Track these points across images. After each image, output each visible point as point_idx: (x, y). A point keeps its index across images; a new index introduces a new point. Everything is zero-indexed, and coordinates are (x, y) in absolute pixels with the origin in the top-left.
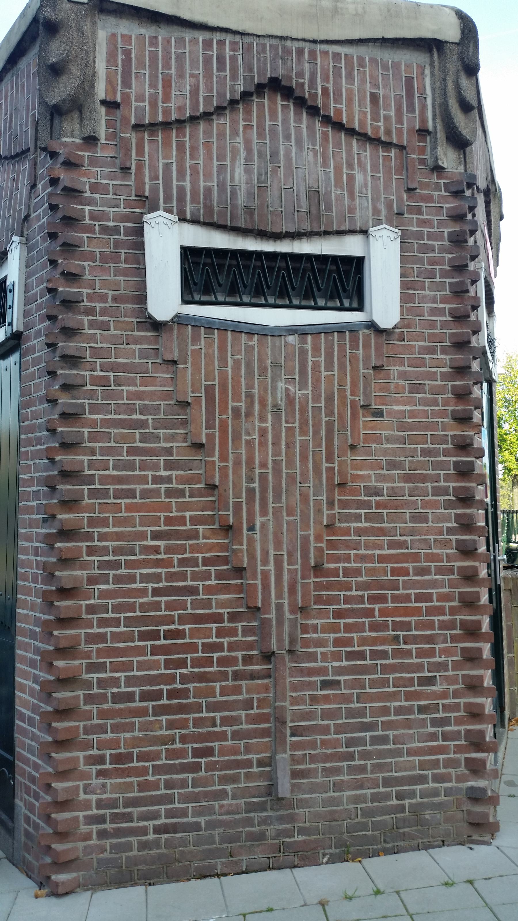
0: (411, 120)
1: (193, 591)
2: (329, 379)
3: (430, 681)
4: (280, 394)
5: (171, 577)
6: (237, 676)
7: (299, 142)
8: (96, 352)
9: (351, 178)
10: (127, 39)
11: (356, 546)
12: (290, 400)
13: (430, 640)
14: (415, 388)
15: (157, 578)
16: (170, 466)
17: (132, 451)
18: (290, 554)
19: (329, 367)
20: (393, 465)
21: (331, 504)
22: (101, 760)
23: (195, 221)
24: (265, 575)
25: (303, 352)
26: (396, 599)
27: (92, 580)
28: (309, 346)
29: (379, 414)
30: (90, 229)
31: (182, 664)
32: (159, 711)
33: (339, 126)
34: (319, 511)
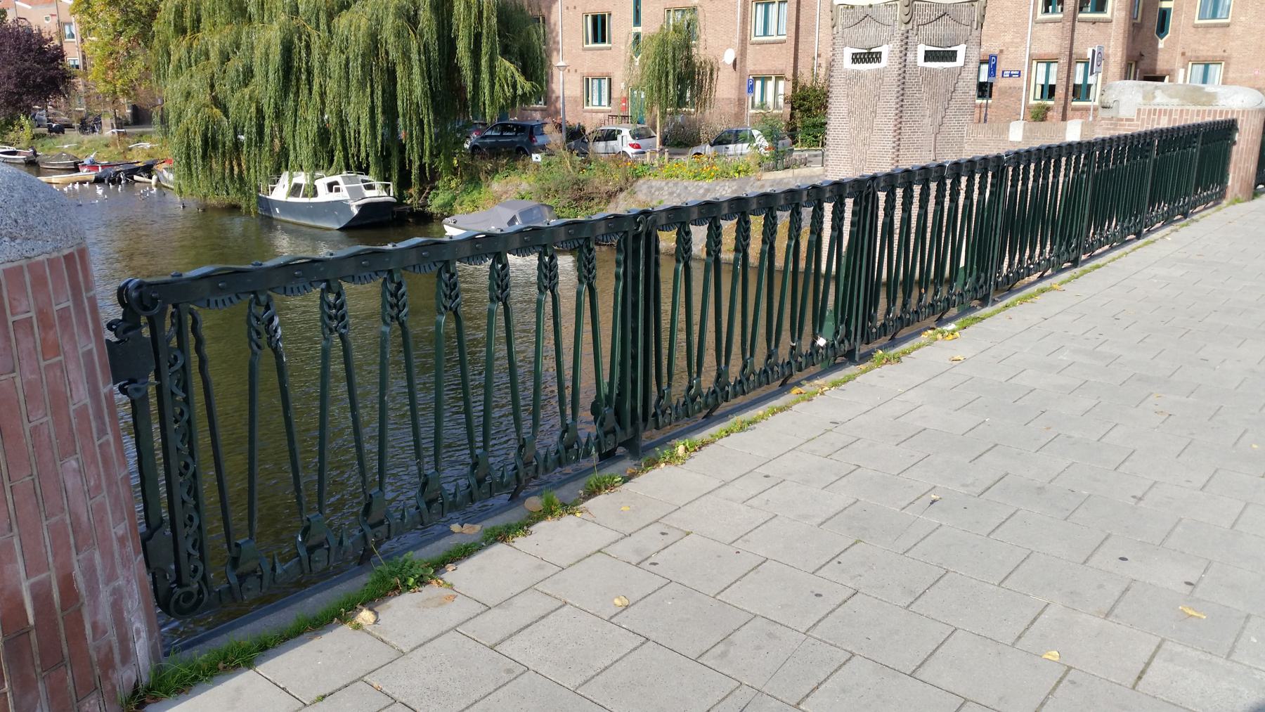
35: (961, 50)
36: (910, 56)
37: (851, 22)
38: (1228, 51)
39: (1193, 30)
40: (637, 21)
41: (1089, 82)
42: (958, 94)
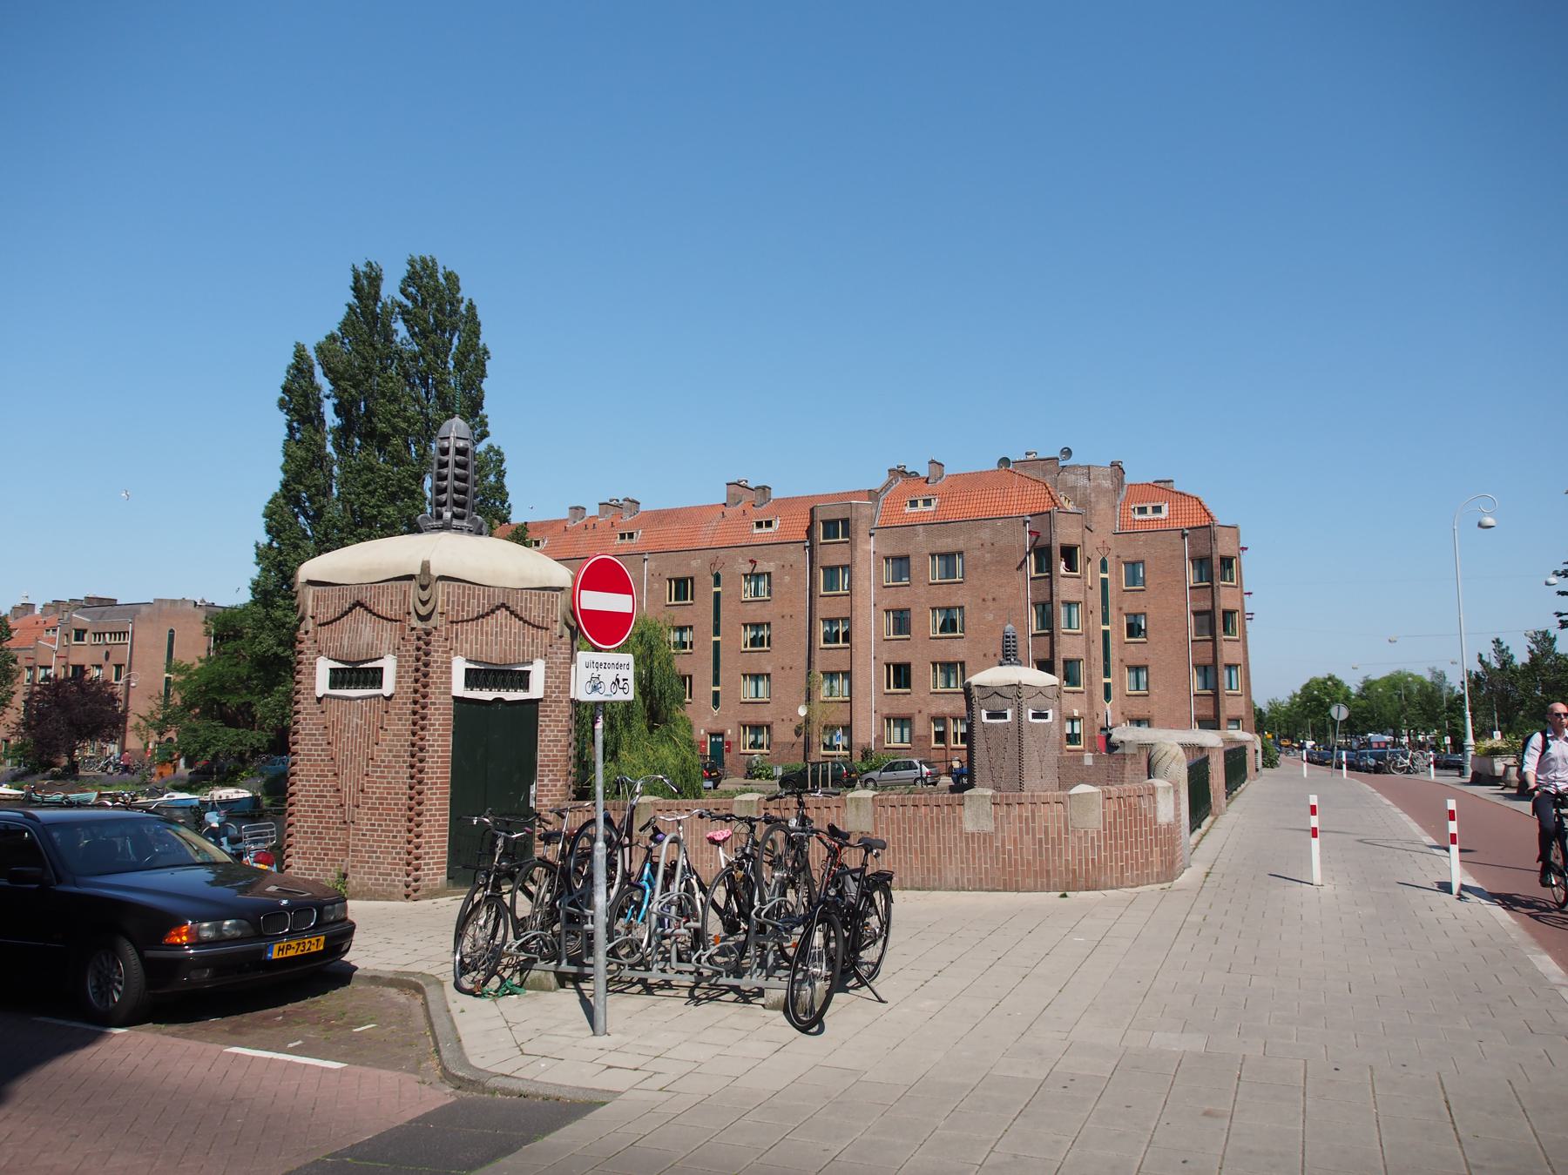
0: (404, 609)
1: (325, 797)
2: (370, 717)
3: (395, 837)
4: (355, 723)
5: (320, 791)
6: (337, 829)
7: (366, 624)
8: (305, 709)
9: (382, 636)
10: (318, 591)
11: (375, 783)
12: (357, 725)
13: (397, 821)
14: (400, 720)
15: (316, 791)
16: (322, 750)
17: (312, 745)
18: (354, 785)
19: (370, 712)
20: (390, 751)
21: (368, 766)
22: (298, 853)
23: (332, 659)
24: (346, 791)
25: (362, 706)
26: (387, 804)
27: (300, 791)
28: (364, 704)
29: (386, 730)
30: (305, 664)
31: (321, 822)
32: (315, 838)
33: (379, 616)
34: (363, 768)
35: (1050, 712)
36: (1024, 716)
37: (985, 696)
38: (1151, 712)
39: (1127, 698)
40: (716, 682)
41: (1075, 732)
42: (1051, 738)
